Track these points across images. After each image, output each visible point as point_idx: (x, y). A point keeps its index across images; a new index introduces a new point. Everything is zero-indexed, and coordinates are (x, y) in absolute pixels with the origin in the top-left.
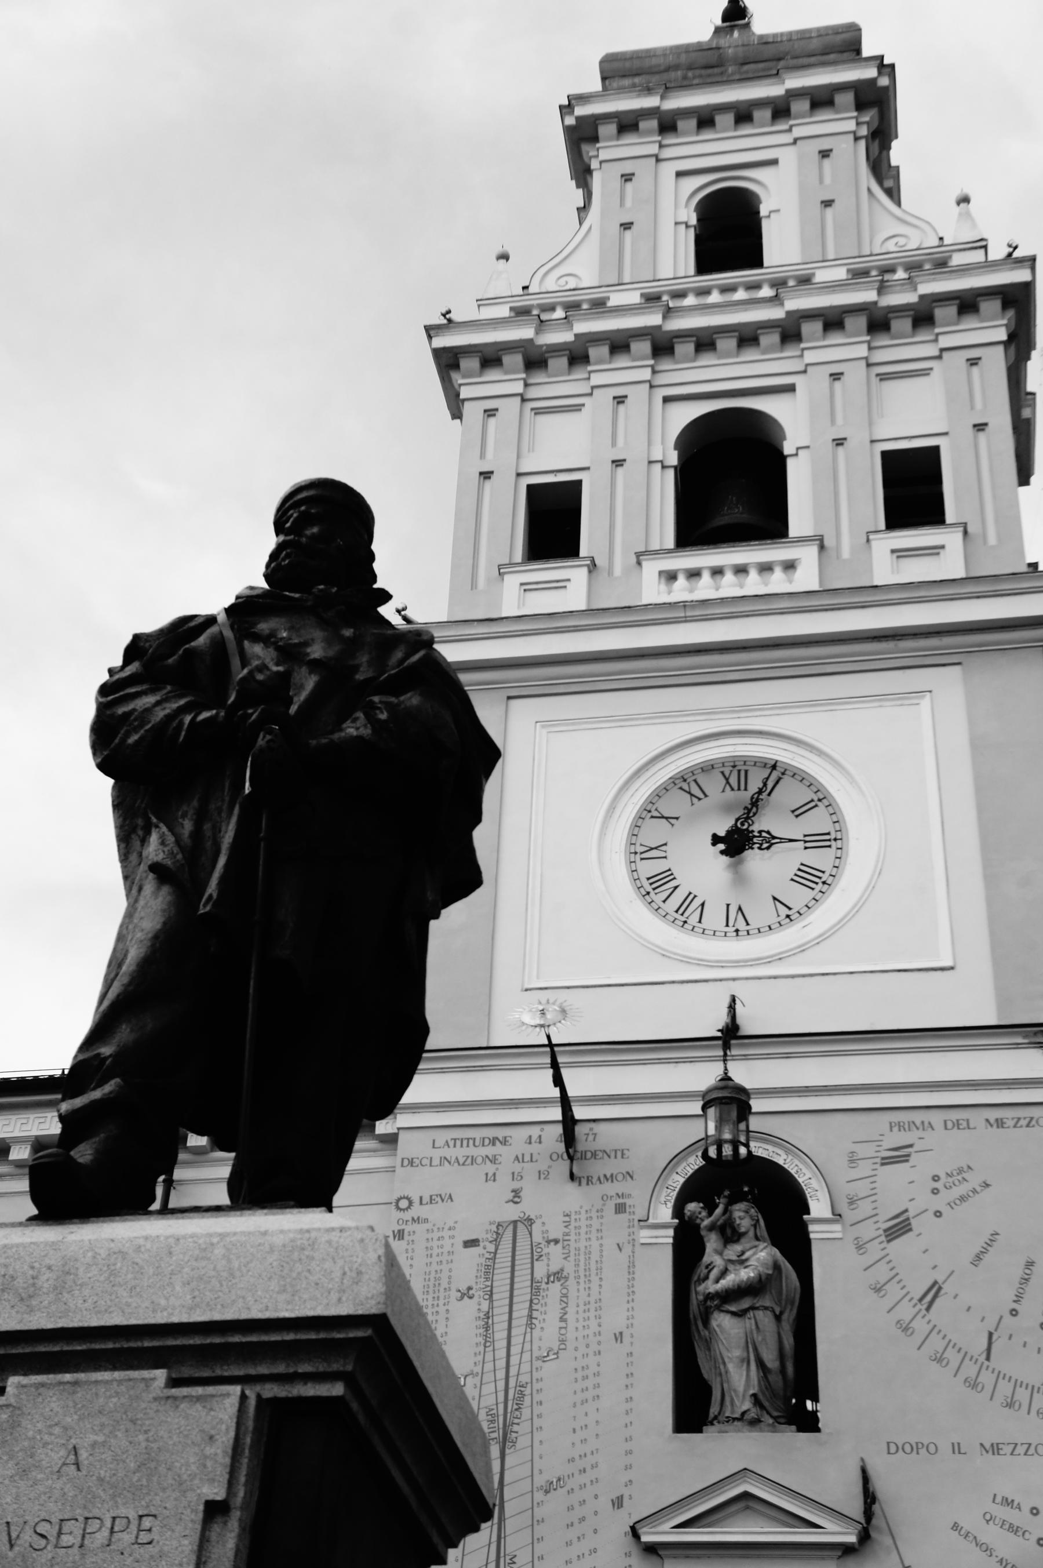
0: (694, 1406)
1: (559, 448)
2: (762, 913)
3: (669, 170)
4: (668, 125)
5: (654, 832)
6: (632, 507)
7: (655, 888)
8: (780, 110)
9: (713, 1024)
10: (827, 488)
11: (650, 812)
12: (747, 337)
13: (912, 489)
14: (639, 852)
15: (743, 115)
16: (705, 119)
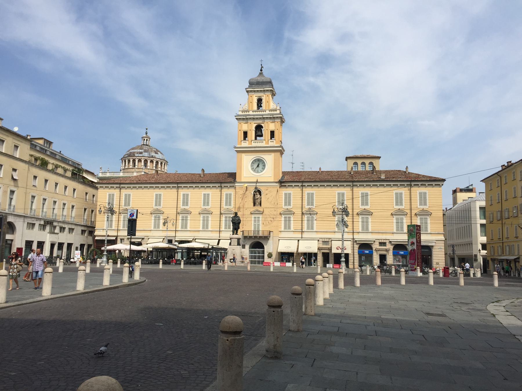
0: (254, 205)
1: (245, 127)
2: (260, 171)
3: (254, 96)
4: (254, 91)
6: (252, 134)
7: (252, 169)
8: (264, 91)
9: (256, 181)
10: (266, 133)
11: (252, 163)
12: (260, 118)
13: (272, 134)
14: (251, 166)
15: (261, 91)
16: (258, 91)
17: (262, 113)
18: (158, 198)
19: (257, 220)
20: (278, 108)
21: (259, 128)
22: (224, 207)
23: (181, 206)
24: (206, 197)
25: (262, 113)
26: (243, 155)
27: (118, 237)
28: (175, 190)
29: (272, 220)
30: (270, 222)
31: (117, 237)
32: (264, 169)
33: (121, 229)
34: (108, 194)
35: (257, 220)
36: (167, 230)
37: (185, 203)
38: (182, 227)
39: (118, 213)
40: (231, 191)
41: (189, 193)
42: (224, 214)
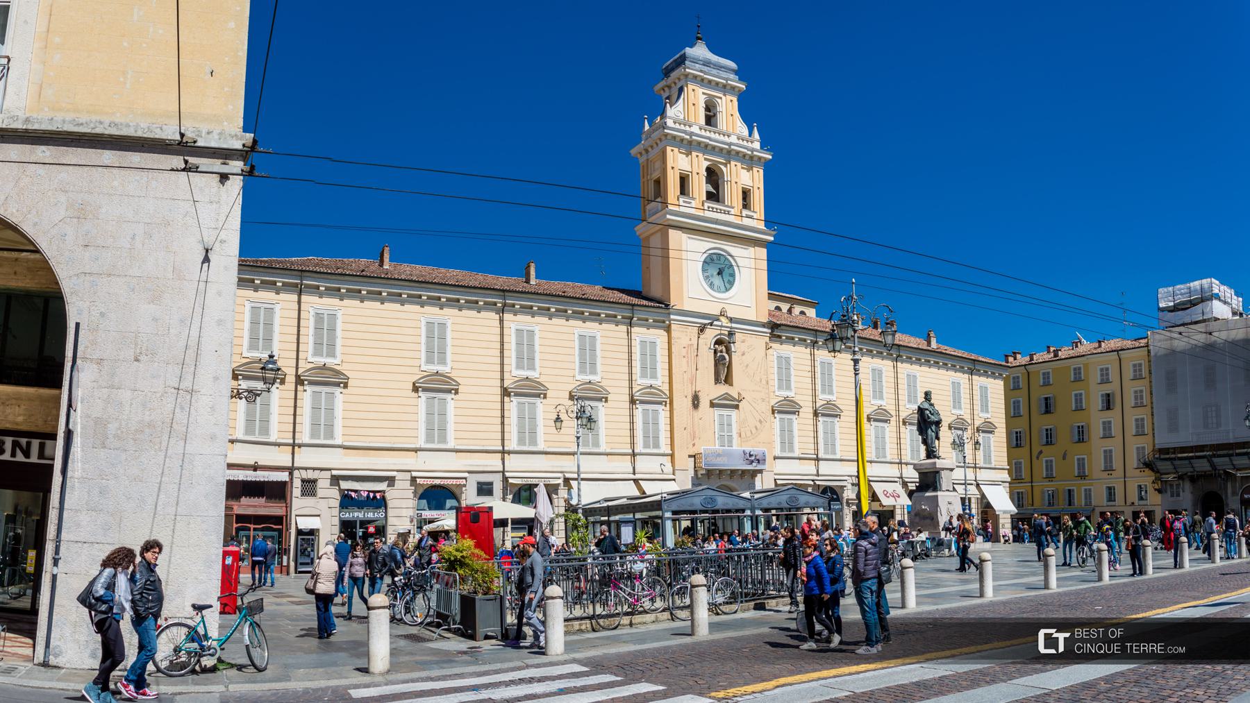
5: (706, 267)
6: (700, 186)
14: (704, 270)
17: (717, 136)
18: (436, 335)
19: (725, 425)
20: (756, 135)
21: (713, 175)
22: (639, 382)
23: (514, 373)
24: (587, 348)
25: (717, 136)
26: (684, 236)
27: (296, 473)
28: (491, 317)
29: (758, 425)
30: (754, 431)
31: (291, 470)
32: (731, 283)
33: (307, 440)
34: (248, 306)
35: (725, 425)
36: (672, 456)
37: (527, 358)
38: (521, 441)
39: (291, 379)
40: (659, 336)
41: (537, 329)
42: (642, 402)
